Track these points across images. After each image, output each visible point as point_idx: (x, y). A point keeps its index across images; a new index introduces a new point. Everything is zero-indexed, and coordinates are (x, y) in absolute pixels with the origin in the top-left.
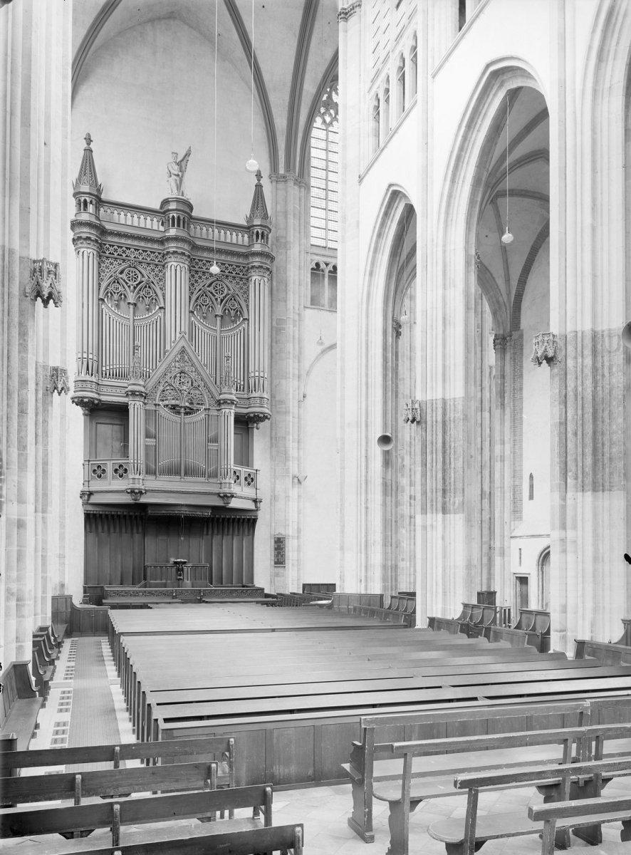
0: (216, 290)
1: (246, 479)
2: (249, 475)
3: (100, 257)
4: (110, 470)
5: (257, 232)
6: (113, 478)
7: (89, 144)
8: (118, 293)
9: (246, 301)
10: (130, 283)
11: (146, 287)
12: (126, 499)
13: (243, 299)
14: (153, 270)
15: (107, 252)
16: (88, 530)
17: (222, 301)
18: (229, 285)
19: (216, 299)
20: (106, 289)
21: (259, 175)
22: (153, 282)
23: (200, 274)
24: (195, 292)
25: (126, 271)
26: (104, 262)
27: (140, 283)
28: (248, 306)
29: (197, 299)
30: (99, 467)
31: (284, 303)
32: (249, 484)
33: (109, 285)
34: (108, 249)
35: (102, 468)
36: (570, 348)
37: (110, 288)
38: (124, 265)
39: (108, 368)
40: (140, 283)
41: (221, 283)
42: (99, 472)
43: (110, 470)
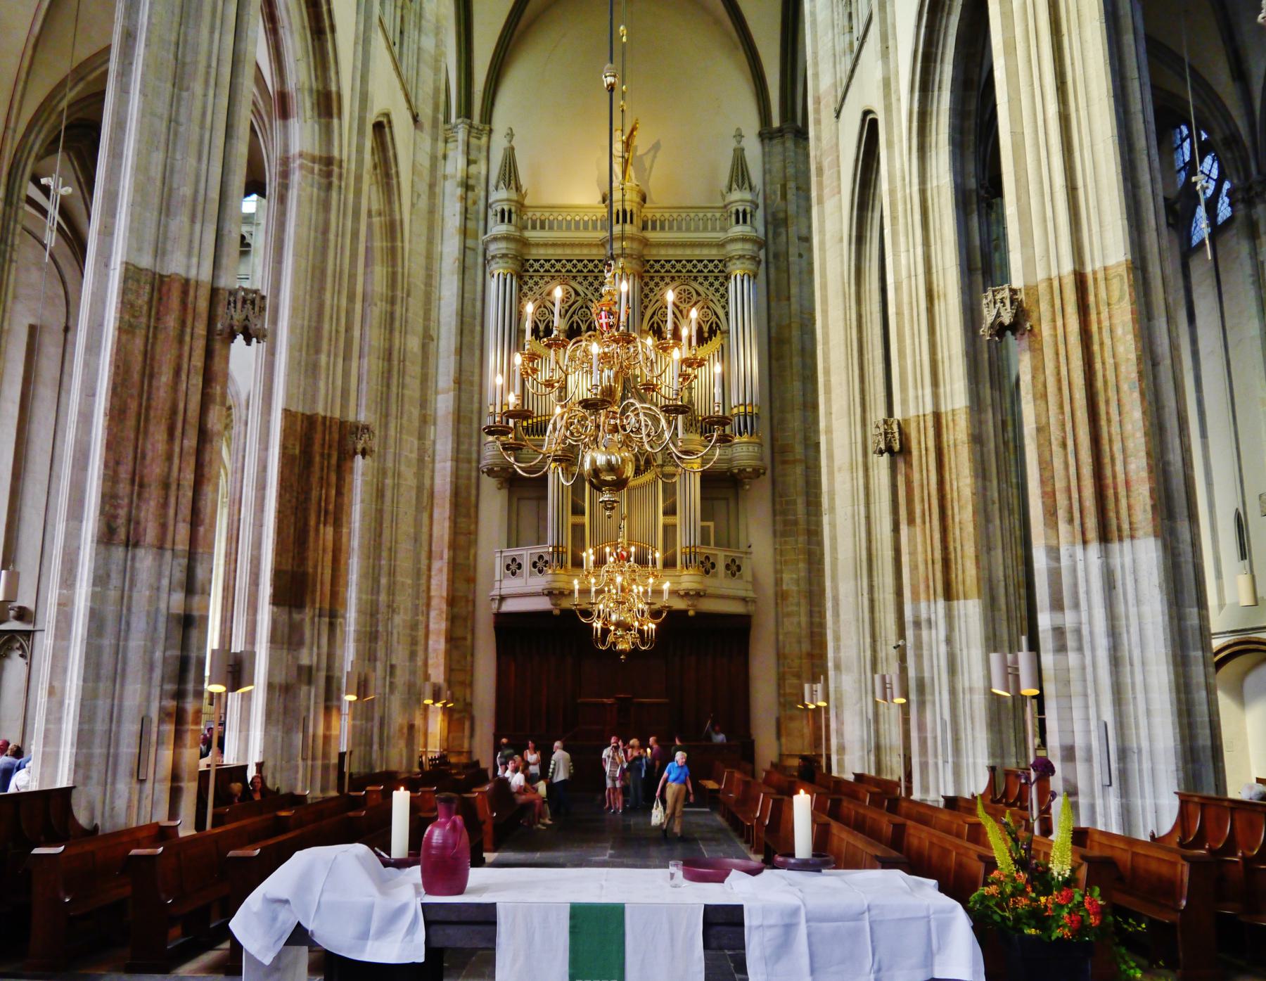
1: (728, 567)
2: (733, 561)
3: (520, 277)
5: (737, 211)
7: (510, 141)
9: (724, 307)
11: (582, 307)
12: (543, 604)
13: (719, 306)
14: (591, 284)
18: (700, 289)
21: (739, 136)
24: (650, 306)
26: (526, 283)
27: (574, 303)
28: (727, 314)
29: (654, 314)
30: (514, 560)
31: (786, 303)
32: (733, 575)
34: (532, 266)
35: (518, 561)
36: (1044, 307)
40: (574, 303)
41: (687, 287)
42: (513, 567)
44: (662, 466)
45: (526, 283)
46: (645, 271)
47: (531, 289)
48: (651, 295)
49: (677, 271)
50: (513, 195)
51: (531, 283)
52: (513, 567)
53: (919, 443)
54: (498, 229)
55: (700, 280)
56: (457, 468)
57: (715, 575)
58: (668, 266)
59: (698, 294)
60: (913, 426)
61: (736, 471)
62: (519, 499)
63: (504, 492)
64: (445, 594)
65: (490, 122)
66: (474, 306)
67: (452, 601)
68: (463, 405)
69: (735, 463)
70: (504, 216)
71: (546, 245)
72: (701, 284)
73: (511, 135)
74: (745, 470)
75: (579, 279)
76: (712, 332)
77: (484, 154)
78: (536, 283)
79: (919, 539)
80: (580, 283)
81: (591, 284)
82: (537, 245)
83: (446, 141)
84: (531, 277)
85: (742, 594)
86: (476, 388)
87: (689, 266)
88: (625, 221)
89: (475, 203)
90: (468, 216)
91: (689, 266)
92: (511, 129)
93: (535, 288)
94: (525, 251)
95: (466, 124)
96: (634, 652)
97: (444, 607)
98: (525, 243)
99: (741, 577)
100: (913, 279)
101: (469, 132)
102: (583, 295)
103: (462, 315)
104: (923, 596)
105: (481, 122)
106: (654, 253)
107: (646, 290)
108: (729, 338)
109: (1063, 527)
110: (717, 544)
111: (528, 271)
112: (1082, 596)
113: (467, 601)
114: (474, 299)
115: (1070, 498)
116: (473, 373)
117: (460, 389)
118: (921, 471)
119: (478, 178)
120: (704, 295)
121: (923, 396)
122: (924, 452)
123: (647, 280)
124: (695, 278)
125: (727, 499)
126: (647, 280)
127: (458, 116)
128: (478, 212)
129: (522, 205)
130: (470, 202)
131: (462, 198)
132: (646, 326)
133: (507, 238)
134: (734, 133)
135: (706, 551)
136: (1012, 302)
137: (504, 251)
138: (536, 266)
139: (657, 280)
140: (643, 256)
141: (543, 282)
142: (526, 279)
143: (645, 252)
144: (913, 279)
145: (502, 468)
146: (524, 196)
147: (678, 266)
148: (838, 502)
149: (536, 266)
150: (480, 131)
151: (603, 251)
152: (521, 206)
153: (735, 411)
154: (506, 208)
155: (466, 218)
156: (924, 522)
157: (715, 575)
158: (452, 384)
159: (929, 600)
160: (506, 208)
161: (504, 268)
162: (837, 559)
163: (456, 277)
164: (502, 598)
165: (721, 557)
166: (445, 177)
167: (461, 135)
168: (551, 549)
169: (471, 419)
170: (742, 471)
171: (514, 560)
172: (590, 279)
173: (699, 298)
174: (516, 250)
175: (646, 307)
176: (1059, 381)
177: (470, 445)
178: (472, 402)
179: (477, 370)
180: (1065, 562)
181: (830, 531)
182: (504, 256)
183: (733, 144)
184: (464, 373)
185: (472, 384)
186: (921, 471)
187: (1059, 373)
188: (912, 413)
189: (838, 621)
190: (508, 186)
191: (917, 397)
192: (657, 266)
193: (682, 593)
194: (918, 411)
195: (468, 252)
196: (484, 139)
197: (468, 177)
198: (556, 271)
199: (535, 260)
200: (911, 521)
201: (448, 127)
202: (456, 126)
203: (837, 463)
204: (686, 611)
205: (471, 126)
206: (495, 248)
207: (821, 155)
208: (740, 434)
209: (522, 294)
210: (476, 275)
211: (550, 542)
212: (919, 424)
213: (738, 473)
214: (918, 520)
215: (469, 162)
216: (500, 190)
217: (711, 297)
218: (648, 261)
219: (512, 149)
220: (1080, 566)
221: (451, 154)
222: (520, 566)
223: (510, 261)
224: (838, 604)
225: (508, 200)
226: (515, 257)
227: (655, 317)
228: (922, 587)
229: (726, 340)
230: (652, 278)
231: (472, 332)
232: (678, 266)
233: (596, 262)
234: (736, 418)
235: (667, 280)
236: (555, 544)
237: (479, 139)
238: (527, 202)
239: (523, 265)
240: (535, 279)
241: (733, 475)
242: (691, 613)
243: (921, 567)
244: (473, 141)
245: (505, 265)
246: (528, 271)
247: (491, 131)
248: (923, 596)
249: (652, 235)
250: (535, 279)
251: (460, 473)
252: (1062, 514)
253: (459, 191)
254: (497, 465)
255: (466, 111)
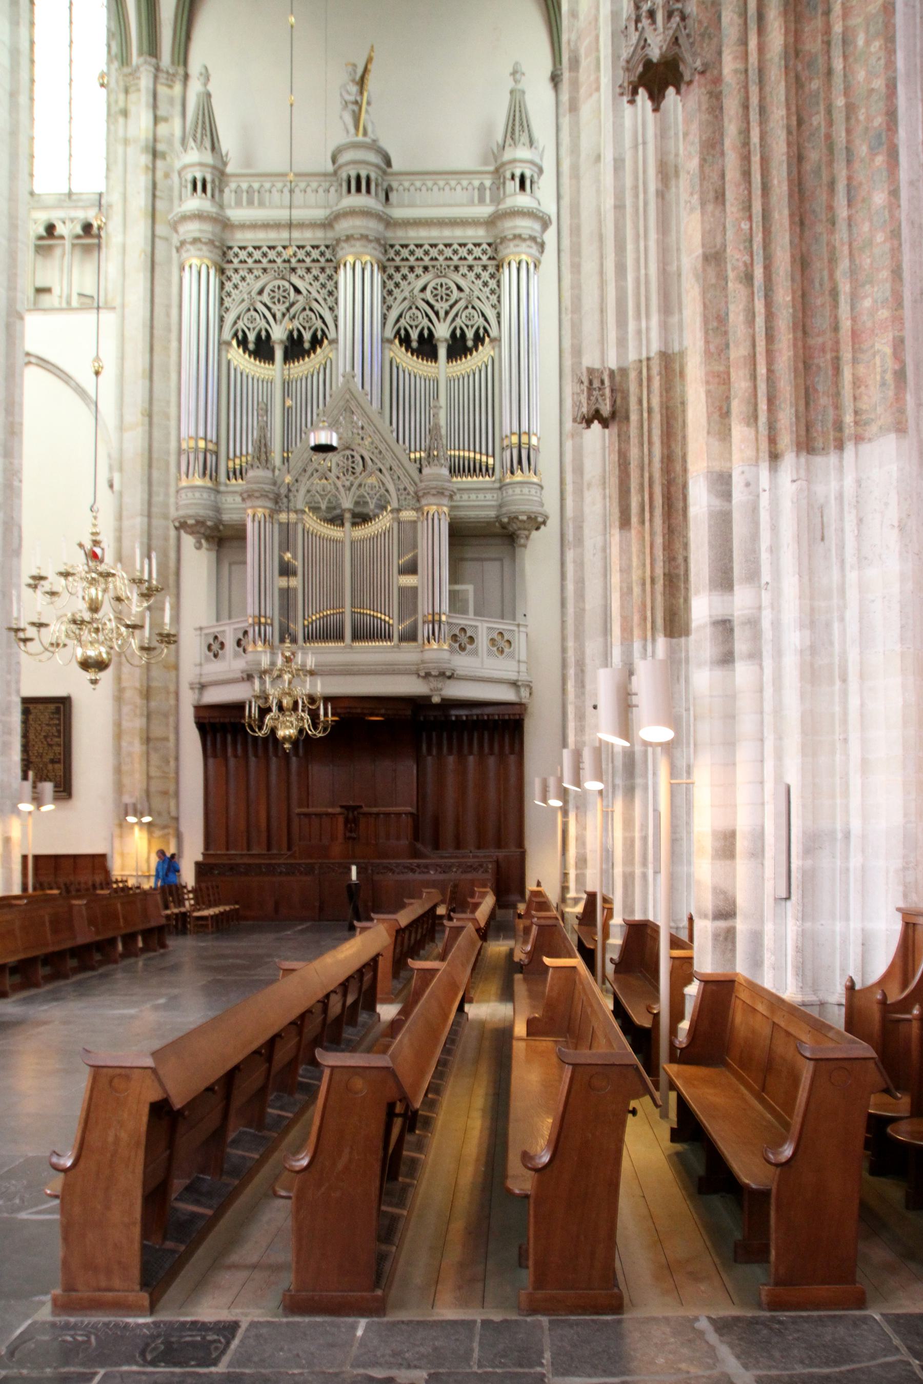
0: (436, 295)
3: (222, 271)
4: (230, 643)
6: (236, 655)
7: (205, 85)
8: (254, 329)
10: (275, 308)
13: (488, 304)
15: (236, 261)
16: (209, 752)
17: (447, 313)
19: (437, 314)
20: (235, 323)
22: (316, 300)
23: (405, 271)
24: (395, 306)
25: (267, 291)
26: (229, 279)
29: (400, 316)
33: (238, 318)
35: (220, 639)
37: (240, 325)
38: (264, 279)
39: (237, 461)
41: (444, 280)
42: (215, 647)
43: (230, 643)
44: (398, 510)
45: (229, 279)
46: (389, 260)
47: (236, 287)
48: (396, 292)
49: (432, 259)
50: (208, 158)
51: (236, 278)
52: (215, 647)
53: (640, 402)
54: (195, 203)
55: (463, 270)
56: (149, 525)
57: (475, 653)
58: (419, 253)
59: (460, 289)
60: (633, 375)
61: (505, 520)
62: (230, 564)
63: (213, 555)
64: (138, 685)
65: (186, 64)
66: (168, 315)
67: (147, 694)
68: (155, 445)
69: (504, 510)
70: (199, 186)
71: (254, 226)
72: (464, 276)
73: (206, 76)
74: (517, 518)
75: (299, 272)
76: (479, 339)
77: (178, 108)
78: (243, 279)
79: (635, 549)
80: (302, 277)
81: (316, 278)
82: (243, 226)
83: (127, 91)
84: (236, 270)
85: (513, 676)
86: (173, 423)
87: (448, 252)
88: (359, 190)
89: (167, 176)
90: (158, 193)
91: (448, 252)
92: (206, 69)
93: (242, 285)
94: (227, 235)
95: (150, 64)
96: (302, 741)
97: (138, 700)
98: (225, 225)
99: (512, 656)
100: (640, 148)
101: (156, 78)
102: (304, 292)
103: (152, 327)
104: (636, 632)
105: (173, 63)
106: (399, 236)
107: (390, 285)
108: (500, 347)
109: (739, 431)
110: (476, 614)
111: (231, 262)
112: (765, 556)
113: (168, 693)
114: (168, 307)
115: (754, 377)
116: (168, 402)
117: (151, 424)
118: (641, 445)
119: (170, 142)
120: (467, 290)
121: (648, 329)
122: (645, 415)
123: (391, 271)
124: (456, 268)
125: (501, 560)
126: (391, 271)
127: (140, 53)
128: (171, 189)
129: (222, 173)
130: (159, 174)
131: (147, 167)
132: (389, 333)
133: (199, 216)
134: (511, 70)
135: (462, 621)
136: (670, 15)
137: (197, 235)
138: (243, 255)
139: (405, 271)
140: (385, 238)
141: (252, 276)
142: (230, 273)
143: (389, 234)
144: (640, 148)
145: (198, 522)
146: (225, 164)
147: (434, 252)
148: (587, 531)
149: (243, 255)
150: (171, 77)
151: (330, 234)
152: (221, 174)
153: (506, 442)
154: (199, 177)
155: (154, 196)
156: (642, 522)
157: (475, 653)
158: (140, 415)
159: (645, 639)
160: (199, 177)
161: (200, 257)
162: (583, 610)
163: (141, 275)
164: (202, 687)
165: (483, 629)
166: (126, 142)
167: (145, 81)
168: (250, 621)
169: (167, 464)
170: (514, 519)
171: (216, 638)
172: (315, 272)
173: (462, 295)
174: (213, 234)
175: (389, 308)
176: (746, 158)
177: (167, 495)
178: (167, 441)
179: (173, 399)
180: (739, 494)
181: (575, 571)
182: (196, 241)
183: (510, 84)
184: (155, 403)
185: (167, 417)
186: (641, 445)
187: (746, 143)
188: (632, 356)
189: (583, 694)
190: (200, 146)
191: (639, 332)
192: (405, 253)
193: (422, 674)
194: (640, 353)
195: (157, 240)
196: (178, 88)
197: (155, 140)
198: (270, 261)
199: (240, 248)
200: (625, 522)
201: (126, 70)
202: (138, 67)
203: (587, 477)
204: (428, 698)
205: (158, 69)
206: (192, 229)
207: (579, 38)
208: (512, 473)
209: (224, 294)
210: (170, 272)
211: (250, 611)
212: (641, 372)
213: (509, 523)
214: (634, 520)
215: (156, 120)
216: (190, 151)
217: (477, 293)
218: (392, 246)
219: (209, 95)
220: (764, 501)
221: (132, 109)
222: (222, 645)
223: (204, 248)
224: (583, 671)
225: (201, 164)
226: (211, 242)
227: (402, 321)
228: (636, 618)
229: (497, 349)
230: (397, 269)
231: (167, 349)
232: (434, 252)
233: (323, 248)
234: (508, 452)
235: (419, 271)
236: (257, 613)
237: (170, 87)
238: (229, 169)
239: (224, 254)
240: (242, 273)
241: (504, 526)
242: (436, 699)
243: (637, 590)
244: (162, 90)
245: (198, 253)
246: (231, 262)
247: (186, 77)
248: (636, 632)
249: (398, 213)
250: (242, 273)
251: (154, 532)
252: (737, 407)
253: (144, 159)
254: (190, 517)
255: (152, 48)
